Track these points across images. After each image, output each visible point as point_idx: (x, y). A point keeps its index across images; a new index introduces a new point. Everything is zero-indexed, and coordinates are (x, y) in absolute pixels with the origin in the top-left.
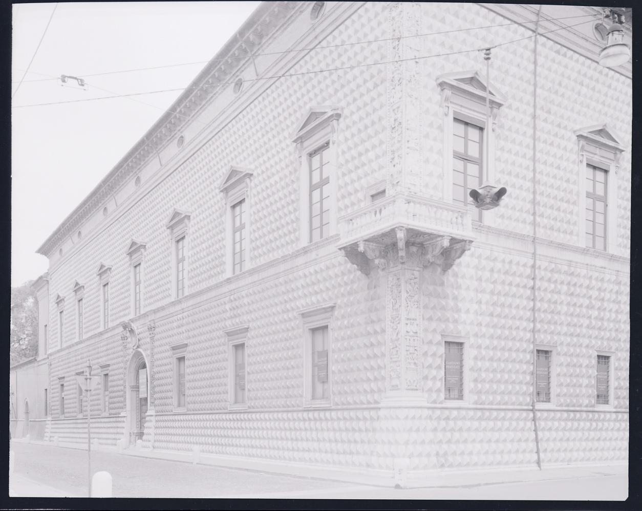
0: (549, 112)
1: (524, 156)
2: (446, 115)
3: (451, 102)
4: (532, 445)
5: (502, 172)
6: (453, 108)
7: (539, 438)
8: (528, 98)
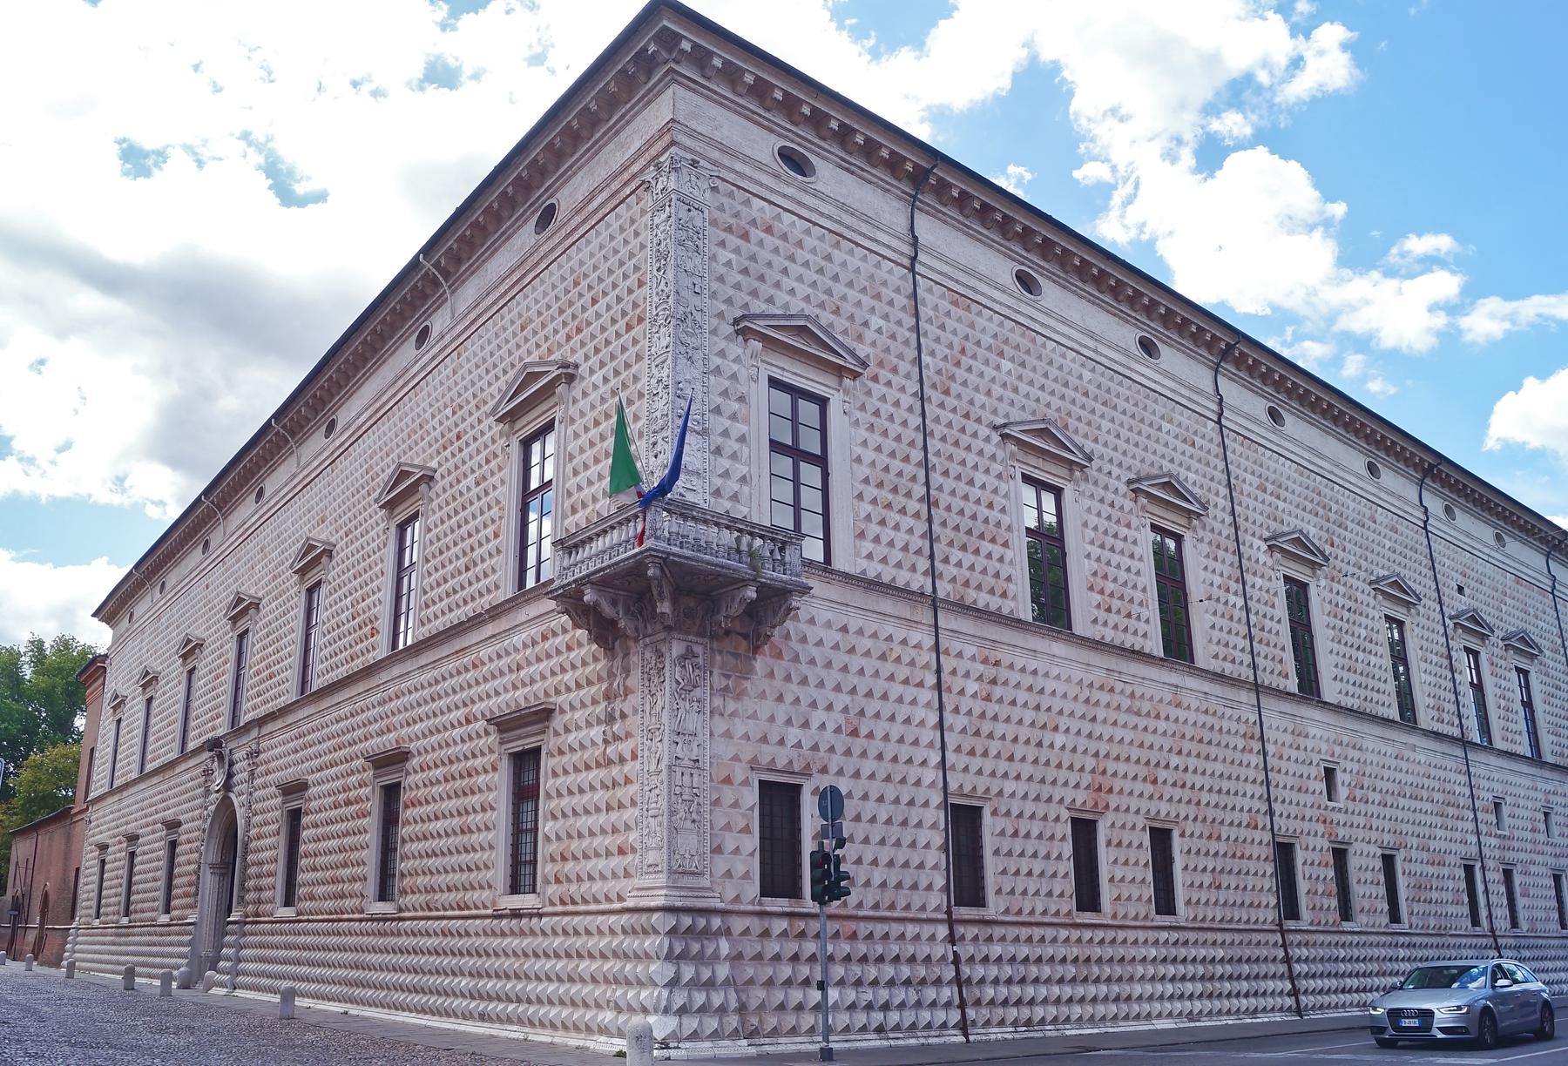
0: (947, 392)
1: (907, 459)
4: (947, 993)
5: (866, 481)
6: (765, 372)
8: (904, 367)
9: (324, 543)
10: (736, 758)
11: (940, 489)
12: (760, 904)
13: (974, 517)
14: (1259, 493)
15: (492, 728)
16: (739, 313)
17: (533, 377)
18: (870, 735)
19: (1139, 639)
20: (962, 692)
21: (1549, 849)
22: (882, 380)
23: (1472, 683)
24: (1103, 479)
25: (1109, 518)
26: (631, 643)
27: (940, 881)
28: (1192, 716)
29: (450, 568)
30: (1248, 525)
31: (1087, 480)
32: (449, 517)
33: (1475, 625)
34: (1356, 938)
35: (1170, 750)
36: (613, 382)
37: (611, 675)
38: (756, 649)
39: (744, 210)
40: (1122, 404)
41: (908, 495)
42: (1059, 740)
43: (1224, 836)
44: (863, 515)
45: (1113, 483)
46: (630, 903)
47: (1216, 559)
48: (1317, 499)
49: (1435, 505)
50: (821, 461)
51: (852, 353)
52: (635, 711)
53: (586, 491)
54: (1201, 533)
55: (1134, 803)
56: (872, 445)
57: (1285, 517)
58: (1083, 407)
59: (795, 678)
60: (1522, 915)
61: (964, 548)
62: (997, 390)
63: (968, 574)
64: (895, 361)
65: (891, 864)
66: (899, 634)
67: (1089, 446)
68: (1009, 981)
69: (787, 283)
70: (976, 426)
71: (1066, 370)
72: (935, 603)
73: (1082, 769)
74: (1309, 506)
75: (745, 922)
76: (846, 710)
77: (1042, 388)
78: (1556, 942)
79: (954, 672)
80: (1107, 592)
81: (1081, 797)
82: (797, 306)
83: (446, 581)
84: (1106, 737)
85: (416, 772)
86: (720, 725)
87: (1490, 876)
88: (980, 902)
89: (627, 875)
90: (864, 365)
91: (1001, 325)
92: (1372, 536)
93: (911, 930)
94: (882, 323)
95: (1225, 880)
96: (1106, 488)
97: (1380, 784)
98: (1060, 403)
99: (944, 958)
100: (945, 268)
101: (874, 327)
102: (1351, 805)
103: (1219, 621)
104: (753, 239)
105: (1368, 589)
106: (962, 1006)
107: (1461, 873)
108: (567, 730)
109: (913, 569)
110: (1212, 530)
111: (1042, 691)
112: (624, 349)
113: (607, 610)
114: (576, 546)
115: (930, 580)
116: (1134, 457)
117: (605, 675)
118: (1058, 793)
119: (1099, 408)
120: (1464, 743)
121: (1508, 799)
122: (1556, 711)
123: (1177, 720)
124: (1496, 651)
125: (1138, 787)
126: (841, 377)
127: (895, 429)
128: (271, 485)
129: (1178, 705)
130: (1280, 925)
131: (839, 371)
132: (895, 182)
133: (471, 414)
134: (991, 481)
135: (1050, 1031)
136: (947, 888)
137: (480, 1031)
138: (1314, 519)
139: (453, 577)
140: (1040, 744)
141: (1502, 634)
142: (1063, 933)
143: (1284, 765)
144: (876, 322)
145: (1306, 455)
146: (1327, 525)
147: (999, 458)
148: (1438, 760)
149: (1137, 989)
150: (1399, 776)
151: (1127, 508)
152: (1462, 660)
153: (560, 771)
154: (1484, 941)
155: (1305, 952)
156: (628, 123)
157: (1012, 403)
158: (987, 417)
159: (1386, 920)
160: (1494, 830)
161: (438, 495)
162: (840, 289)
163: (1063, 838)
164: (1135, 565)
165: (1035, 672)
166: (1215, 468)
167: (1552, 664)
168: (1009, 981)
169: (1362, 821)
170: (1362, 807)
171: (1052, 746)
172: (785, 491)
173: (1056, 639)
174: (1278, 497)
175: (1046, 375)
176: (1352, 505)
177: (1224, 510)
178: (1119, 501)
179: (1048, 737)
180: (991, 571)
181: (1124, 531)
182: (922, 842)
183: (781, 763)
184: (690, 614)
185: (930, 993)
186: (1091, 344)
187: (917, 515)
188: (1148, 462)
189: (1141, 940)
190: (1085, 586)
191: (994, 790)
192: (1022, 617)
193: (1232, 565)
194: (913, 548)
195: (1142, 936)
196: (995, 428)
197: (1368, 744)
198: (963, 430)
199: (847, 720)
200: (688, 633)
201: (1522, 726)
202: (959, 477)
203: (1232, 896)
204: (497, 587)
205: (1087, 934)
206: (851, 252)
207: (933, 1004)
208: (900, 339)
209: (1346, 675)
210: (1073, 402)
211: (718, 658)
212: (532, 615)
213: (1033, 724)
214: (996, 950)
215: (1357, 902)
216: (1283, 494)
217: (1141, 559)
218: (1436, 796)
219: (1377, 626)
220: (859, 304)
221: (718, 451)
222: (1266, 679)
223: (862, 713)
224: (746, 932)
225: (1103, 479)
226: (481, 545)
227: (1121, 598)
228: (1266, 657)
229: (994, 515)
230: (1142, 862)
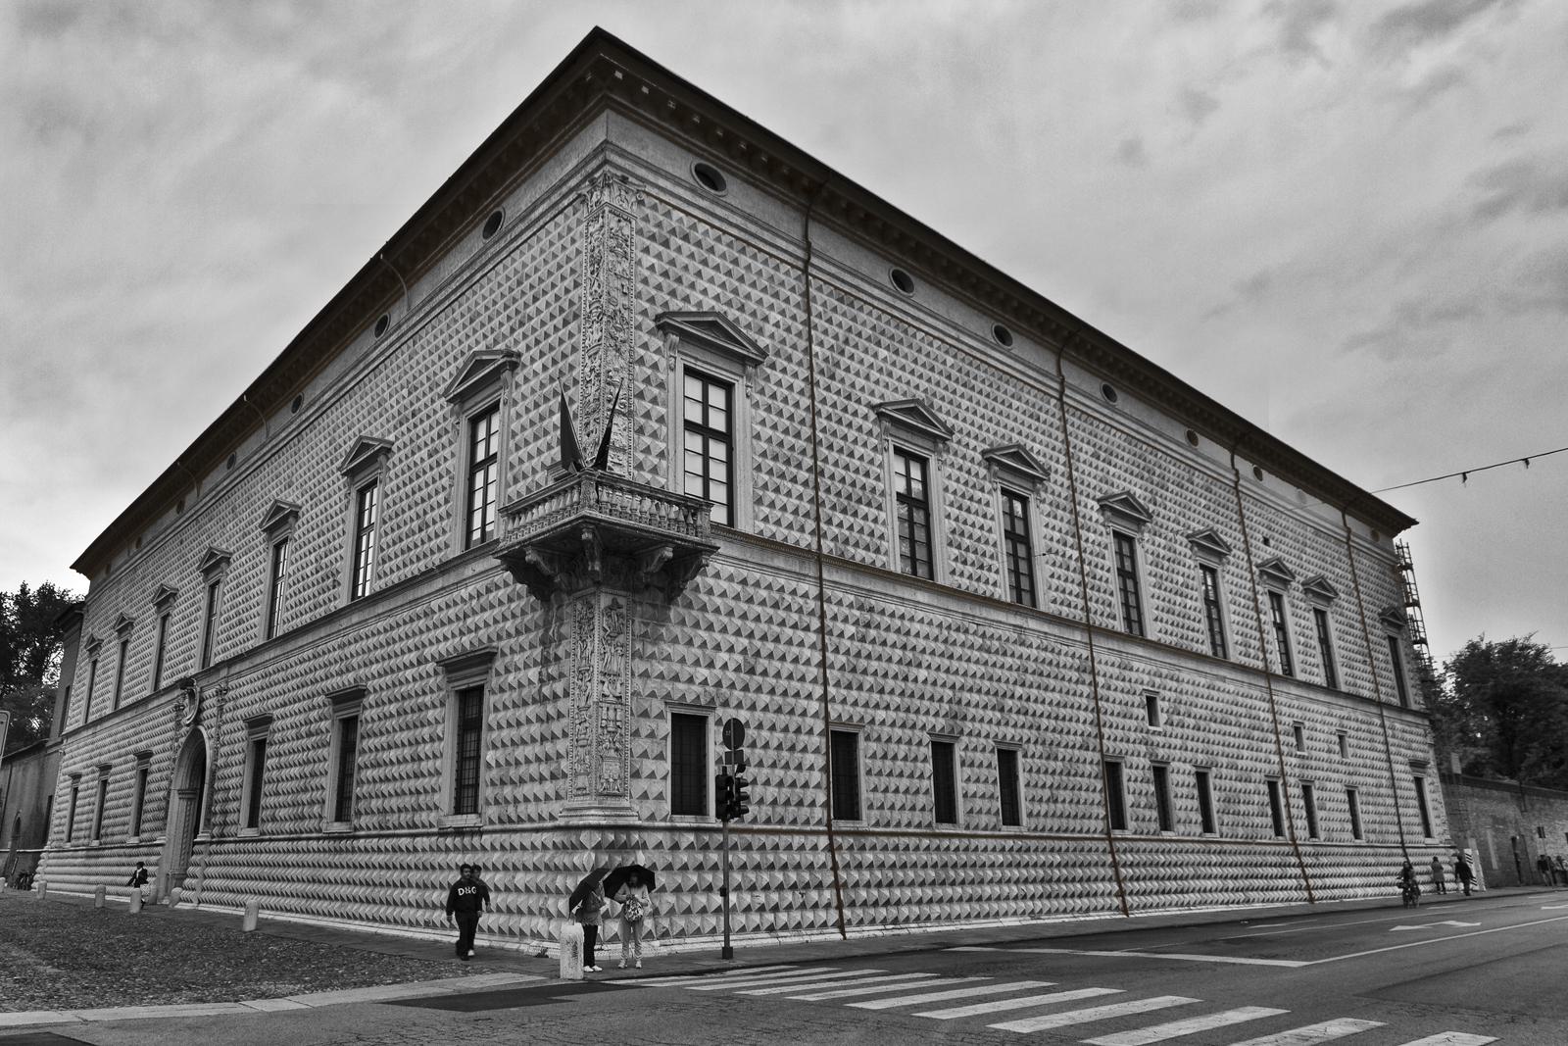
0: (832, 377)
1: (798, 435)
2: (673, 369)
4: (828, 895)
5: (764, 454)
7: (841, 882)
8: (798, 355)
9: (290, 505)
10: (653, 695)
11: (825, 460)
12: (671, 821)
13: (853, 484)
14: (1095, 462)
15: (440, 669)
16: (660, 311)
17: (480, 364)
18: (765, 673)
19: (990, 587)
20: (841, 635)
21: (1343, 768)
22: (779, 367)
23: (1275, 623)
24: (962, 450)
25: (966, 483)
26: (565, 596)
27: (821, 798)
28: (1034, 652)
29: (405, 529)
30: (1083, 488)
31: (948, 451)
32: (405, 484)
33: (1276, 574)
34: (1174, 846)
35: (1015, 683)
36: (551, 370)
37: (547, 624)
38: (670, 600)
40: (979, 385)
41: (799, 466)
42: (923, 674)
43: (1060, 757)
44: (761, 484)
45: (970, 453)
46: (561, 822)
47: (1055, 517)
48: (1143, 464)
49: (1245, 467)
50: (727, 437)
51: (754, 344)
52: (568, 655)
53: (527, 464)
54: (1043, 495)
55: (985, 728)
56: (769, 423)
57: (1115, 480)
58: (946, 388)
59: (703, 625)
60: (1320, 825)
61: (844, 511)
62: (874, 375)
63: (847, 533)
64: (790, 351)
65: (780, 784)
66: (788, 589)
67: (950, 421)
68: (879, 885)
69: (701, 284)
70: (856, 406)
71: (932, 356)
72: (819, 558)
73: (941, 700)
74: (1136, 471)
75: (660, 836)
76: (744, 652)
77: (912, 372)
78: (1351, 850)
79: (835, 618)
80: (964, 546)
81: (940, 723)
82: (709, 303)
83: (401, 540)
84: (961, 672)
85: (371, 706)
86: (640, 666)
87: (1291, 791)
88: (855, 815)
89: (558, 797)
90: (764, 353)
91: (879, 318)
92: (1190, 496)
93: (797, 840)
94: (779, 317)
95: (1062, 794)
96: (964, 457)
97: (1194, 710)
98: (927, 385)
99: (824, 865)
100: (833, 270)
101: (772, 321)
102: (1169, 729)
103: (1059, 571)
104: (673, 246)
105: (1185, 541)
106: (840, 907)
107: (1264, 788)
108: (507, 671)
109: (802, 529)
110: (1053, 493)
111: (908, 633)
113: (545, 568)
114: (519, 512)
115: (816, 539)
116: (988, 431)
117: (541, 623)
118: (922, 719)
119: (960, 389)
120: (1267, 674)
121: (1307, 724)
122: (1350, 646)
123: (1021, 657)
124: (1297, 594)
125: (989, 714)
126: (744, 366)
127: (788, 409)
128: (241, 454)
129: (1022, 644)
130: (1108, 834)
131: (743, 360)
133: (425, 394)
134: (869, 453)
135: (914, 929)
136: (826, 805)
137: (426, 936)
138: (1140, 482)
139: (407, 536)
140: (906, 679)
141: (1302, 580)
142: (926, 842)
143: (1112, 694)
144: (774, 317)
145: (1134, 426)
146: (1150, 487)
147: (875, 433)
148: (1245, 690)
149: (988, 890)
150: (1211, 703)
151: (981, 475)
152: (1264, 601)
153: (500, 706)
154: (1286, 849)
155: (1130, 857)
157: (887, 386)
158: (865, 397)
159: (1199, 829)
160: (1294, 751)
161: (395, 465)
162: (745, 289)
163: (925, 760)
164: (988, 523)
165: (902, 617)
166: (1056, 439)
167: (1346, 605)
168: (879, 885)
169: (1178, 742)
170: (1179, 730)
171: (916, 680)
172: (696, 465)
173: (920, 588)
174: (1110, 463)
175: (915, 361)
176: (1173, 469)
177: (1063, 475)
178: (975, 468)
179: (913, 672)
180: (867, 531)
181: (978, 495)
182: (806, 764)
183: (689, 699)
185: (814, 895)
186: (954, 333)
187: (805, 484)
188: (1000, 434)
189: (990, 848)
190: (945, 543)
191: (867, 719)
192: (892, 569)
193: (1069, 522)
194: (802, 512)
195: (991, 843)
196: (873, 407)
197: (1185, 675)
198: (845, 410)
199: (745, 660)
200: (614, 588)
201: (1319, 660)
202: (841, 451)
203: (1068, 808)
204: (447, 546)
205: (946, 843)
206: (754, 257)
207: (816, 906)
208: (794, 331)
209: (1165, 616)
210: (938, 384)
212: (478, 570)
213: (900, 662)
214: (869, 857)
215: (1177, 814)
216: (1114, 460)
217: (992, 519)
218: (1243, 721)
219: (1192, 573)
220: (760, 302)
221: (641, 431)
222: (1098, 620)
223: (758, 654)
224: (659, 846)
225: (962, 450)
226: (432, 509)
227: (975, 552)
228: (1097, 602)
229: (871, 482)
230: (991, 780)
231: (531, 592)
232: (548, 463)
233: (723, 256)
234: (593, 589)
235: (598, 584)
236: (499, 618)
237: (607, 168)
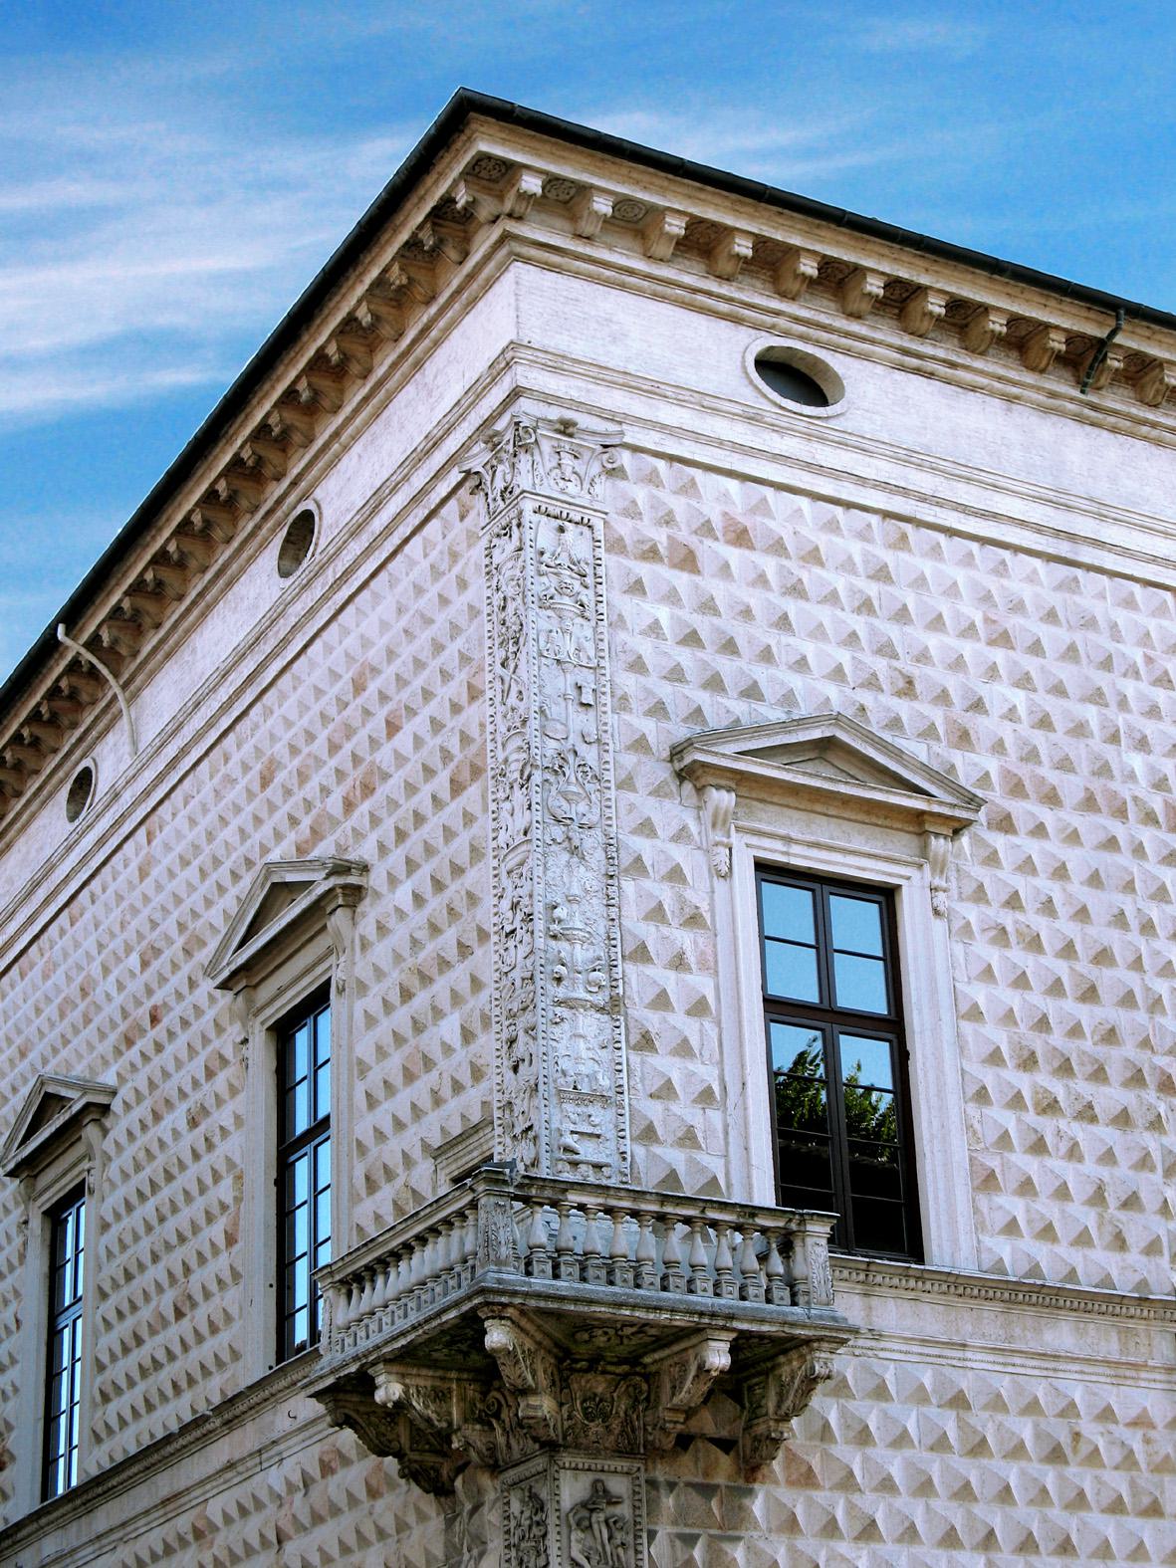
3: (738, 829)
16: (681, 732)
26: (485, 1480)
39: (678, 505)
90: (973, 802)
112: (449, 834)
126: (923, 834)
132: (1029, 378)
144: (1001, 694)
156: (437, 343)
184: (596, 1409)
211: (669, 1502)
221: (646, 1043)
231: (412, 1473)
232: (436, 1141)
233: (848, 566)
234: (540, 1463)
235: (551, 1447)
236: (351, 1540)
237: (524, 405)
